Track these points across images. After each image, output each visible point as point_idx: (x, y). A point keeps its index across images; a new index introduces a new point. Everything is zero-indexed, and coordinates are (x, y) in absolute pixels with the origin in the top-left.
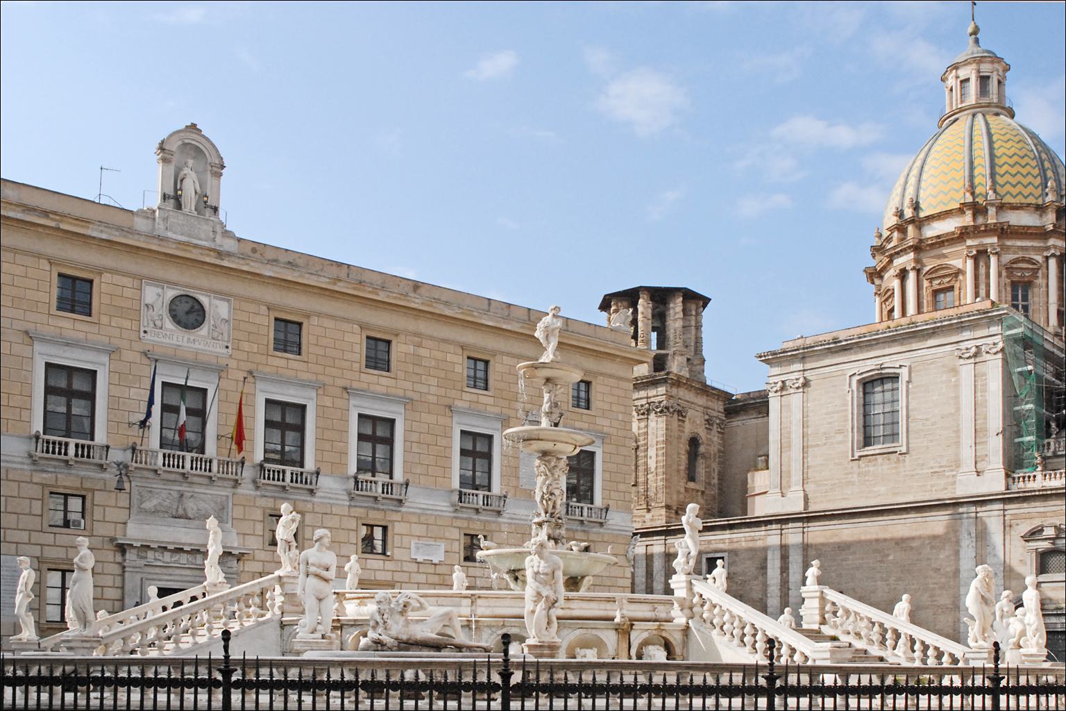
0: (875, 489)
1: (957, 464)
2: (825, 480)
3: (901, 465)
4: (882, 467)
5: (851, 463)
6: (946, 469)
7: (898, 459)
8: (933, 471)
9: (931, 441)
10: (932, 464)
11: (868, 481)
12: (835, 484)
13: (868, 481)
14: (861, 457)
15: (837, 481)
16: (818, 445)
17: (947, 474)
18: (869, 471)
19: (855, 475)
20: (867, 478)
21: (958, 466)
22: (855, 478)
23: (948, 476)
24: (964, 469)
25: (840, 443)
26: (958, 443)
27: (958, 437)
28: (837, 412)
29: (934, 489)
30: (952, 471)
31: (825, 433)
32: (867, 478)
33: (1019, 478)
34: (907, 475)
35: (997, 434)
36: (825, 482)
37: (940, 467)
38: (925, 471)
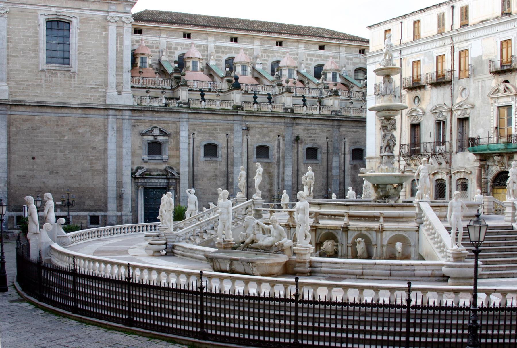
0: (56, 93)
2: (22, 81)
3: (72, 79)
4: (60, 78)
5: (40, 73)
7: (70, 75)
9: (91, 68)
10: (91, 82)
11: (51, 86)
12: (29, 85)
13: (51, 86)
14: (47, 69)
15: (30, 83)
16: (17, 56)
17: (100, 90)
18: (52, 80)
19: (43, 81)
20: (51, 84)
21: (106, 86)
22: (43, 83)
23: (101, 92)
24: (109, 88)
25: (33, 58)
26: (106, 73)
27: (107, 69)
28: (31, 37)
29: (92, 98)
30: (103, 88)
31: (22, 49)
32: (51, 84)
34: (76, 87)
35: (128, 71)
36: (23, 83)
37: (96, 85)
38: (87, 86)
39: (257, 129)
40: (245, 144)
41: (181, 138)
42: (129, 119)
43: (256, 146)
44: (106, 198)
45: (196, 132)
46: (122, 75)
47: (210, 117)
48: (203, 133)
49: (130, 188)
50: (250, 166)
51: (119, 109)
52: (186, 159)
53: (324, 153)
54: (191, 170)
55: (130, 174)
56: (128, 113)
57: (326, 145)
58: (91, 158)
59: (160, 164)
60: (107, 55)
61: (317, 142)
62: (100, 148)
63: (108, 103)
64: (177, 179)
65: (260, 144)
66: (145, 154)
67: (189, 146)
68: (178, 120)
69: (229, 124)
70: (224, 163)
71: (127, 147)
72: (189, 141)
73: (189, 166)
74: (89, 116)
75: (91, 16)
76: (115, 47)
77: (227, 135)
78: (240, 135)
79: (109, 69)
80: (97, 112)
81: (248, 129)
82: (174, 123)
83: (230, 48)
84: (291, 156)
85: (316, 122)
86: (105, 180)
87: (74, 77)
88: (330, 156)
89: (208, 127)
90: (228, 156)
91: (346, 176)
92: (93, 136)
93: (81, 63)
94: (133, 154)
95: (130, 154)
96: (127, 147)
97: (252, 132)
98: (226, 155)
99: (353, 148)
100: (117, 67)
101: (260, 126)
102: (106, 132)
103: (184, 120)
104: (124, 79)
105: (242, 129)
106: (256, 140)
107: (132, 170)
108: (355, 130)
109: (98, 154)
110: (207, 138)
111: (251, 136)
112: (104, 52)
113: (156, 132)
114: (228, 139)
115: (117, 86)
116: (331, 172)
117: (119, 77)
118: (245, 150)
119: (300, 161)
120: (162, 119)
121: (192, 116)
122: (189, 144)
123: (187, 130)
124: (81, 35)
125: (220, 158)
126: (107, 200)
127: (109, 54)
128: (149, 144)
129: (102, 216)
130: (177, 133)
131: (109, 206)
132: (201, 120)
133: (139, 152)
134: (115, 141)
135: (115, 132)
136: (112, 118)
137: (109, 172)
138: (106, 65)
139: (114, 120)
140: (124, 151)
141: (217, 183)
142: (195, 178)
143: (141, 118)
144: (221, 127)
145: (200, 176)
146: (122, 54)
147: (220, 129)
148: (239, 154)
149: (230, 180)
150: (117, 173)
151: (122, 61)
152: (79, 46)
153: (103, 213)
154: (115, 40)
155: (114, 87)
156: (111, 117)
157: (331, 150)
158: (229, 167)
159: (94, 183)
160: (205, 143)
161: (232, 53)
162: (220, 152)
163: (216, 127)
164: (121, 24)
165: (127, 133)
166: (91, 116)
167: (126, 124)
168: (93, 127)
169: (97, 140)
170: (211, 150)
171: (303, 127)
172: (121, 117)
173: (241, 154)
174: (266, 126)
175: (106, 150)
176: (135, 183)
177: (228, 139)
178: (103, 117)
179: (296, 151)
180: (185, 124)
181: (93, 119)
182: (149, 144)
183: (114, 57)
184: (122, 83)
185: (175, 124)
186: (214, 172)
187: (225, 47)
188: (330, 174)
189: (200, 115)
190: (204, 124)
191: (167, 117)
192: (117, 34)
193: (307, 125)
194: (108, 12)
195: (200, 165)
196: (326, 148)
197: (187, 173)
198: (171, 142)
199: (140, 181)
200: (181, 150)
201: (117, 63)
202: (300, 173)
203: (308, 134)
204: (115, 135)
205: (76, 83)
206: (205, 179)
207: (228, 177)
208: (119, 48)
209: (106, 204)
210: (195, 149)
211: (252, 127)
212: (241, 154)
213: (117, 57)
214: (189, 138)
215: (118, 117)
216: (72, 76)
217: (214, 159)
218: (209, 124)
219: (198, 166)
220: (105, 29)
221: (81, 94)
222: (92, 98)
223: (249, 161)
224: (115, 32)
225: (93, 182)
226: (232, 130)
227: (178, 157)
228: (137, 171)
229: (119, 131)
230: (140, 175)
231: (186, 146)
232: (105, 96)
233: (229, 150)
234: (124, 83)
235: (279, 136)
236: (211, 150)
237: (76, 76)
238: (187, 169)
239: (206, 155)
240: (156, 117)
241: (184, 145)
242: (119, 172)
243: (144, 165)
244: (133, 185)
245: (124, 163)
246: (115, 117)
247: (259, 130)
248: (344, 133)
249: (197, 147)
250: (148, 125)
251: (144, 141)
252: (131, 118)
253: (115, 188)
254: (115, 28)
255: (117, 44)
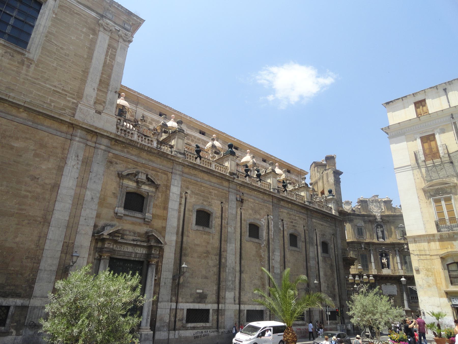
1: (80, 95)
3: (24, 68)
6: (68, 94)
8: (55, 89)
9: (61, 66)
10: (56, 83)
17: (68, 98)
23: (69, 101)
26: (84, 81)
27: (86, 77)
29: (53, 104)
30: (74, 99)
33: (121, 130)
35: (116, 92)
37: (63, 90)
38: (48, 86)
39: (249, 203)
40: (239, 217)
41: (171, 194)
42: (105, 151)
43: (248, 222)
44: (35, 271)
45: (189, 192)
46: (106, 93)
47: (206, 177)
48: (197, 194)
49: (87, 256)
50: (243, 245)
51: (94, 133)
52: (175, 224)
53: (303, 241)
54: (180, 240)
55: (91, 233)
56: (105, 141)
57: (304, 234)
58: (23, 193)
59: (140, 224)
60: (91, 62)
61: (297, 228)
62: (47, 181)
63: (77, 117)
64: (161, 249)
65: (253, 221)
66: (121, 206)
67: (180, 208)
68: (170, 170)
69: (225, 191)
70: (217, 237)
71: (94, 188)
72: (181, 201)
73: (177, 234)
74: (39, 127)
75: (78, 9)
76: (103, 57)
77: (222, 203)
78: (234, 206)
79: (89, 79)
80: (56, 125)
81: (242, 201)
82: (165, 173)
83: (199, 139)
84: (279, 240)
85: (296, 207)
86: (43, 237)
87: (28, 67)
88: (308, 245)
89: (202, 189)
90: (221, 229)
91: (320, 269)
92: (37, 159)
93: (47, 54)
94: (102, 202)
95: (96, 201)
96: (94, 188)
97: (245, 205)
98: (220, 227)
99: (322, 241)
100: (100, 81)
101: (252, 200)
102: (64, 159)
103: (178, 172)
104: (108, 98)
105: (237, 200)
106: (249, 216)
107: (95, 226)
108: (321, 223)
109: (39, 190)
110: (201, 201)
111: (244, 210)
112: (85, 56)
113: (142, 177)
114: (222, 208)
115: (95, 103)
116: (309, 263)
117: (100, 93)
118: (239, 224)
119: (286, 246)
120: (151, 163)
121: (186, 170)
122: (180, 204)
123: (180, 186)
124: (56, 21)
125: (213, 229)
126: (35, 276)
127: (94, 61)
128: (128, 194)
129: (16, 307)
130: (168, 187)
131: (37, 287)
132: (196, 179)
133: (112, 201)
134: (77, 175)
135: (80, 163)
136: (79, 141)
137: (53, 222)
138: (86, 72)
139: (82, 145)
140: (89, 194)
141: (208, 263)
142: (184, 251)
143: (122, 154)
144: (216, 192)
145: (189, 250)
146: (112, 70)
147: (215, 194)
148: (233, 228)
149: (223, 260)
150: (67, 227)
151: (110, 76)
152: (49, 32)
153: (19, 302)
154: (105, 51)
155: (92, 103)
156: (77, 139)
157: (307, 240)
158: (223, 242)
159: (17, 240)
160: (198, 207)
161: (200, 143)
162: (214, 222)
163: (211, 191)
164: (117, 38)
165: (98, 168)
166: (44, 128)
167: (99, 156)
168: (42, 145)
169: (44, 167)
170: (204, 218)
171: (286, 211)
172: (93, 145)
173: (235, 228)
174: (257, 202)
175: (56, 187)
176: (96, 248)
177: (222, 208)
178: (63, 135)
179: (282, 235)
180: (178, 177)
181: (46, 134)
182: (128, 194)
183: (100, 68)
184: (104, 102)
185: (167, 175)
186: (206, 247)
187: (195, 137)
188: (309, 264)
189: (196, 172)
190: (199, 183)
191: (158, 163)
192: (109, 45)
193: (289, 210)
194: (102, 16)
195: (190, 235)
196: (304, 237)
197: (174, 244)
198: (158, 197)
199: (106, 246)
200: (170, 210)
201: (101, 77)
202: (286, 260)
203: (290, 218)
204: (79, 166)
205: (30, 74)
206: (195, 255)
207: (220, 255)
208: (108, 61)
209: (31, 283)
210: (186, 212)
211: (246, 200)
212: (235, 228)
213: (103, 70)
214: (181, 197)
215: (89, 143)
216: (26, 63)
217: (207, 229)
218: (204, 185)
219: (188, 236)
220: (95, 33)
221: (34, 91)
222: (53, 104)
223: (242, 238)
224: (107, 42)
225: (16, 237)
226: (227, 199)
227: (165, 219)
228: (103, 228)
229: (87, 163)
230: (110, 234)
231: (176, 206)
232: (75, 109)
233: (223, 221)
234: (107, 103)
235: (268, 215)
236: (204, 218)
237: (33, 67)
238: (174, 238)
239: (198, 223)
240: (144, 158)
241: (173, 205)
242: (72, 227)
243: (115, 222)
244: (92, 252)
245: (83, 213)
246: (85, 141)
247: (251, 205)
248: (315, 224)
249: (189, 210)
250: (130, 166)
251: (121, 186)
252: (109, 149)
253: (58, 254)
254: (108, 38)
255: (107, 55)
